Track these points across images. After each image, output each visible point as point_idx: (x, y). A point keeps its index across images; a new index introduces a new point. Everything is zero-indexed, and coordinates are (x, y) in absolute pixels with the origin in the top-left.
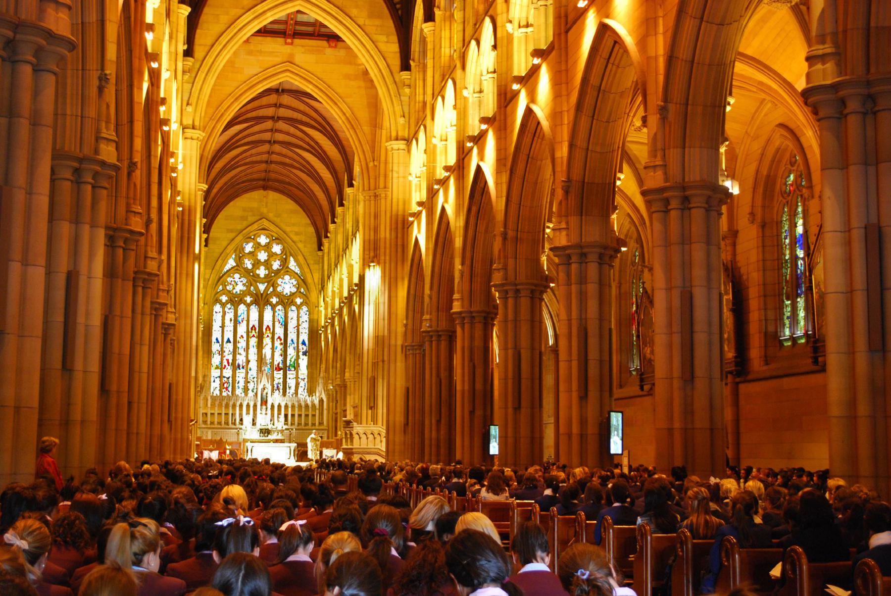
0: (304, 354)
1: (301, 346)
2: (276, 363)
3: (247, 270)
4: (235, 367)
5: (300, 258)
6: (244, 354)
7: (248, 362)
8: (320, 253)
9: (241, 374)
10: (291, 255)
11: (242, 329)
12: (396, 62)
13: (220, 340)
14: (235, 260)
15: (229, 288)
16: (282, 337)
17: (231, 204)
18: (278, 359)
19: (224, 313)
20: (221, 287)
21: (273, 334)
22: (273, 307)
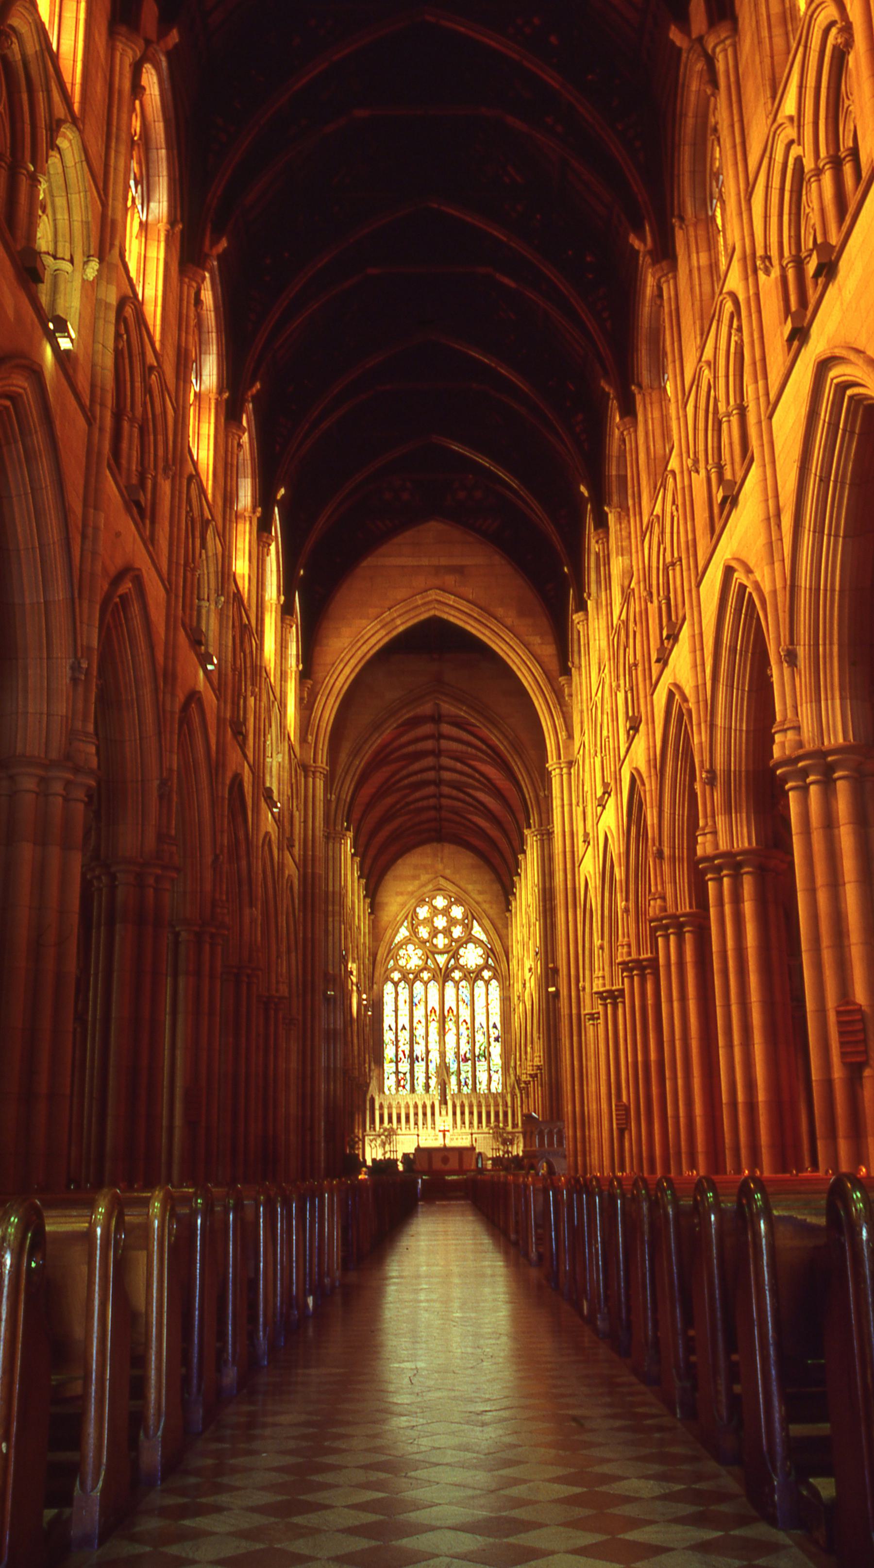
0: (497, 1039)
1: (492, 1030)
2: (462, 1053)
3: (424, 942)
4: (413, 1059)
5: (486, 922)
6: (423, 1043)
7: (428, 1052)
8: (508, 914)
9: (420, 1067)
10: (474, 918)
11: (419, 1013)
12: (553, 665)
13: (393, 1027)
14: (407, 928)
15: (402, 962)
16: (469, 1021)
17: (400, 861)
18: (465, 1048)
19: (397, 993)
20: (392, 963)
21: (458, 1016)
22: (457, 984)
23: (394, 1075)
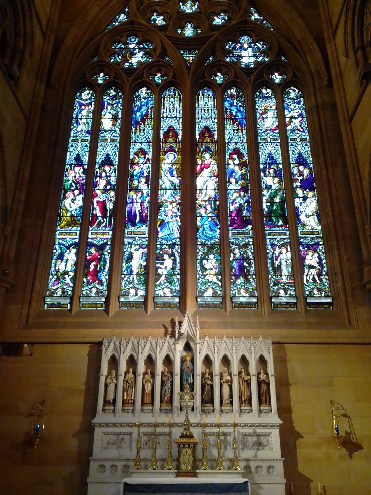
0: (307, 185)
1: (295, 171)
4: (120, 217)
7: (156, 205)
11: (142, 138)
13: (85, 159)
16: (245, 152)
18: (236, 198)
21: (221, 144)
22: (219, 93)
23: (74, 251)
